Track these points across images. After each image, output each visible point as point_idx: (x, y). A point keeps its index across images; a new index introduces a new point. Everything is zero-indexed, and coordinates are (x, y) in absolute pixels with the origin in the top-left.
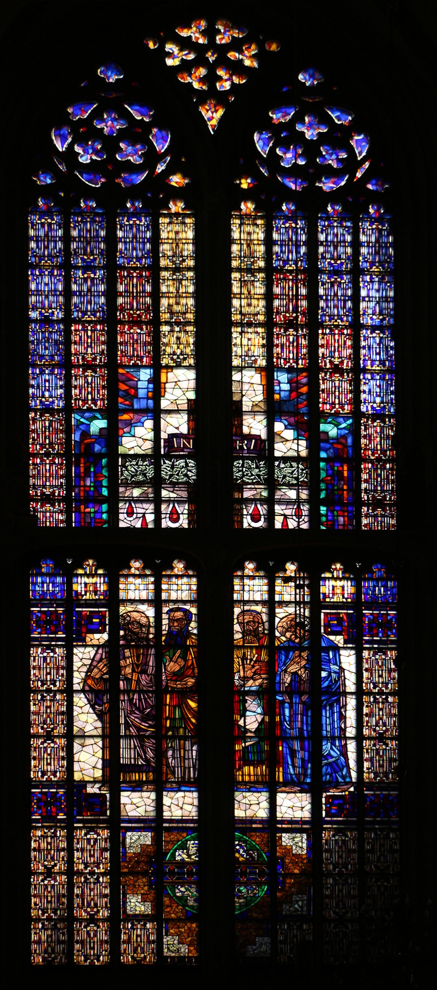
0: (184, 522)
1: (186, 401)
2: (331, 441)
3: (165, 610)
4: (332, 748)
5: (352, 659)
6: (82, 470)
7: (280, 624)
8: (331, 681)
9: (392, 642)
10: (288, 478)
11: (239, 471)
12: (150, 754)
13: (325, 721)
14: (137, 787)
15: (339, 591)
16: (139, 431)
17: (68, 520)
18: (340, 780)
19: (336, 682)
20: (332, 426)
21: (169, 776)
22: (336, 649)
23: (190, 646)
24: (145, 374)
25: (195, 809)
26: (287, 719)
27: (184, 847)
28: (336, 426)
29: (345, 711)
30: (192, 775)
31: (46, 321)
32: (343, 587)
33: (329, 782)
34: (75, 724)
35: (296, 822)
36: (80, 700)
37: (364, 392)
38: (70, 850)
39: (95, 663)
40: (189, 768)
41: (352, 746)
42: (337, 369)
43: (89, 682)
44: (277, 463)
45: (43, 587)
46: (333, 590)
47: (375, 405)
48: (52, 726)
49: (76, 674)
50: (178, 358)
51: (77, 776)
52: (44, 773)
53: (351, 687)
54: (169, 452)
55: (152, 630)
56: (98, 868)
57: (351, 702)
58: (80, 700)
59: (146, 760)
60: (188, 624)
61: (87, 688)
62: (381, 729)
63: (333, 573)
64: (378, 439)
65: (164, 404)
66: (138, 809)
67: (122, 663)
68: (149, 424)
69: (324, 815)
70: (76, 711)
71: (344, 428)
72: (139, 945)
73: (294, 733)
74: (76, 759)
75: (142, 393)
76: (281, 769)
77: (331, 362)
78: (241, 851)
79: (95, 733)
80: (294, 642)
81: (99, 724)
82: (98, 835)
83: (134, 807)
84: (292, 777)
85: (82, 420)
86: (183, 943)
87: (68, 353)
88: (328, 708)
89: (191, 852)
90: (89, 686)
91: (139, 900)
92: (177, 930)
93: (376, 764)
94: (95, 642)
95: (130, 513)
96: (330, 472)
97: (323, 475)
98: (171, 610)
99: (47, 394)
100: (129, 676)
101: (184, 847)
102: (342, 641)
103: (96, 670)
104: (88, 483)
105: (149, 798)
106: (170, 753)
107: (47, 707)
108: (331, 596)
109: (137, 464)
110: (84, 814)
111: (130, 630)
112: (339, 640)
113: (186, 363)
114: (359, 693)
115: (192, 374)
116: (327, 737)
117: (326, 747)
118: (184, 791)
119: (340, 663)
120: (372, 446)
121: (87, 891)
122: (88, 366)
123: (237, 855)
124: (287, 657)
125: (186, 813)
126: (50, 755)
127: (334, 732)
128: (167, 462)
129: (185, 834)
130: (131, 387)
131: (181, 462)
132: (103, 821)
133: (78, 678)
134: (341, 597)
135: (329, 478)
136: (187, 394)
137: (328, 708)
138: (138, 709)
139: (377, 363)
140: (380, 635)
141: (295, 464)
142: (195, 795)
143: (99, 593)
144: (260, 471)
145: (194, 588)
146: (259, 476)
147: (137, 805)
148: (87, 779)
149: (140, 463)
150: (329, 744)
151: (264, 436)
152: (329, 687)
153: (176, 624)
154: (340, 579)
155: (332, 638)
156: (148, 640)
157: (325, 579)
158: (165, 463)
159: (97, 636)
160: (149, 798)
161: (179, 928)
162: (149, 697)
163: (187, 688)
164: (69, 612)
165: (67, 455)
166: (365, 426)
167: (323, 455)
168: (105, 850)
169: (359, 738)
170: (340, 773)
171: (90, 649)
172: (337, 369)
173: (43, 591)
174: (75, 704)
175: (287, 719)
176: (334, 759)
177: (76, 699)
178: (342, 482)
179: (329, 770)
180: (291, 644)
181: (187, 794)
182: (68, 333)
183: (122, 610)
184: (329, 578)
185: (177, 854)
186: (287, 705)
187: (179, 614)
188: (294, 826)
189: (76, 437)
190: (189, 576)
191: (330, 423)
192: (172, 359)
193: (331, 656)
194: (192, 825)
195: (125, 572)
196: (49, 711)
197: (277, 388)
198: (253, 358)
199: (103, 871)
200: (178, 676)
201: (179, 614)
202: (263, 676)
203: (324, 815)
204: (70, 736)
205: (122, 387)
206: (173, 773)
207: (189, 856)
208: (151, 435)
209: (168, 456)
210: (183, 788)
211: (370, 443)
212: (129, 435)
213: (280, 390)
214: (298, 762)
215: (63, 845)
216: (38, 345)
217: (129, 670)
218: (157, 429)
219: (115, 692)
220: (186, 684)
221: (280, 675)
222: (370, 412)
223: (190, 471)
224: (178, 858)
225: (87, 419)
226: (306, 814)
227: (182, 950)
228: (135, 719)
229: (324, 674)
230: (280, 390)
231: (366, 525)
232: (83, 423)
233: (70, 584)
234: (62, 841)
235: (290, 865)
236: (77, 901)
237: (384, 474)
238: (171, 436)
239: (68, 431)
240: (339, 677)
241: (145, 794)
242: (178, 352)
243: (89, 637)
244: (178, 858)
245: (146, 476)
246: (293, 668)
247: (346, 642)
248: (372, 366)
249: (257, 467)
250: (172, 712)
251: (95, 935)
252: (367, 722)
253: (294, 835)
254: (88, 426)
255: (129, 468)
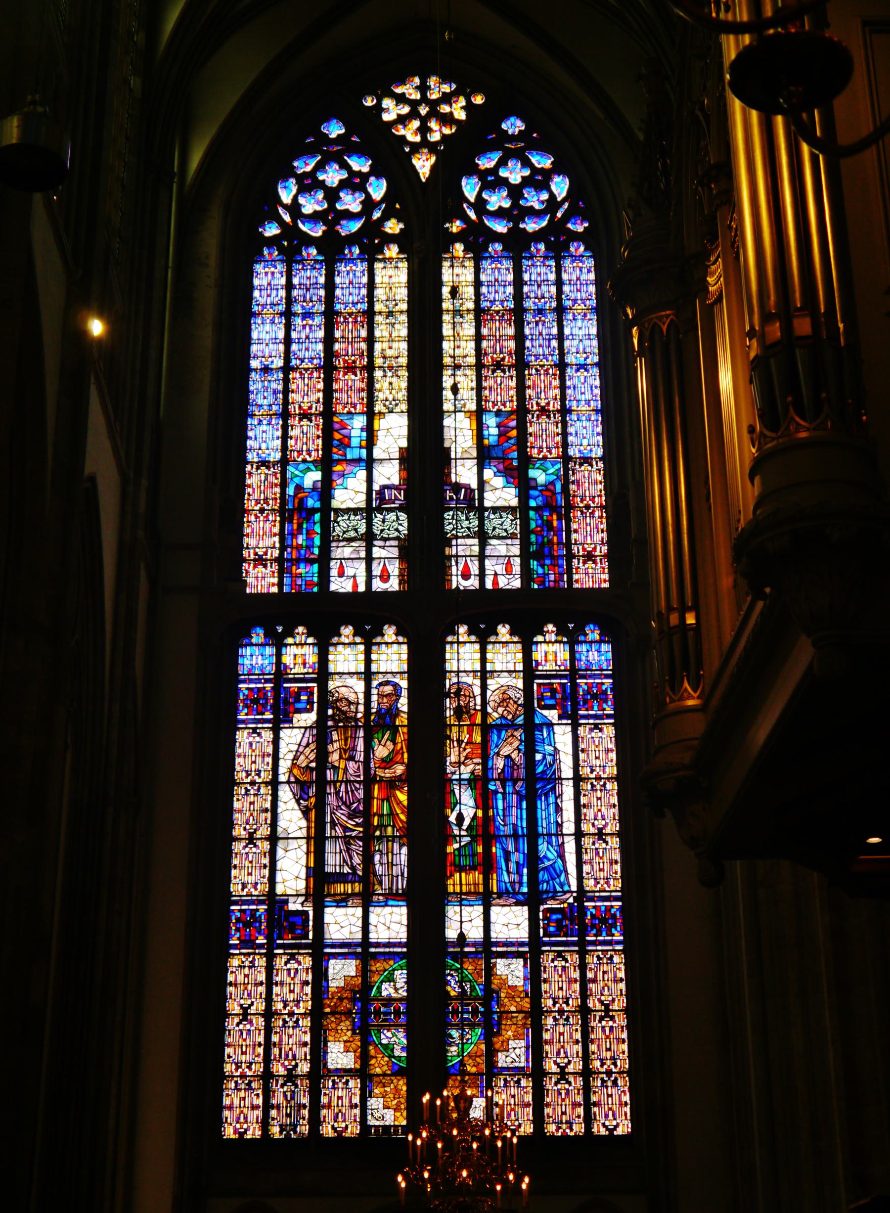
0: (393, 585)
1: (398, 449)
2: (540, 488)
3: (375, 683)
4: (548, 849)
5: (569, 737)
6: (295, 526)
7: (492, 698)
8: (546, 765)
9: (609, 716)
10: (497, 530)
11: (450, 524)
12: (357, 860)
13: (541, 814)
14: (342, 901)
15: (551, 657)
16: (351, 482)
17: (280, 585)
18: (558, 888)
19: (551, 766)
20: (541, 471)
21: (376, 887)
22: (550, 725)
23: (399, 726)
24: (359, 422)
25: (405, 929)
26: (501, 813)
27: (390, 979)
28: (545, 471)
29: (562, 801)
30: (400, 887)
31: (266, 370)
32: (556, 653)
33: (547, 892)
34: (279, 823)
35: (511, 944)
36: (285, 794)
37: (571, 434)
38: (270, 983)
39: (301, 749)
40: (397, 876)
41: (570, 846)
42: (544, 411)
43: (295, 771)
44: (486, 514)
45: (252, 660)
46: (546, 656)
47: (582, 448)
48: (255, 827)
49: (281, 762)
50: (391, 404)
51: (279, 890)
52: (244, 886)
53: (567, 771)
54: (380, 504)
55: (361, 708)
56: (298, 1007)
57: (568, 790)
58: (285, 794)
59: (353, 868)
60: (397, 700)
61: (292, 779)
62: (600, 824)
63: (544, 636)
64: (587, 484)
65: (377, 453)
66: (342, 930)
67: (330, 748)
68: (362, 474)
69: (541, 935)
70: (281, 807)
71: (552, 474)
72: (340, 1111)
73: (509, 830)
74: (278, 867)
75: (355, 442)
76: (495, 875)
77: (538, 404)
78: (453, 982)
79: (299, 834)
80: (506, 718)
81: (304, 823)
82: (299, 963)
83: (338, 927)
84: (506, 887)
85: (297, 472)
86: (389, 1108)
87: (286, 402)
88: (543, 798)
89: (398, 986)
90: (295, 777)
91: (342, 1050)
92: (382, 1090)
93: (596, 867)
94: (303, 724)
95: (341, 574)
96: (540, 522)
97: (533, 525)
98: (381, 684)
99: (264, 446)
100: (336, 764)
101: (390, 979)
102: (556, 717)
103: (302, 757)
104: (300, 542)
105: (353, 915)
106: (377, 858)
107: (251, 803)
108: (543, 663)
109: (349, 519)
110: (285, 937)
111: (339, 709)
112: (552, 715)
113: (397, 409)
114: (578, 779)
115: (404, 420)
116: (543, 835)
117: (543, 847)
118: (392, 906)
119: (555, 743)
120: (580, 493)
121: (285, 1038)
122: (305, 415)
123: (449, 988)
124: (499, 737)
125: (393, 935)
126: (251, 862)
127: (550, 829)
128: (378, 515)
129: (391, 962)
130: (345, 436)
131: (392, 516)
132: (306, 946)
133: (284, 765)
134: (554, 664)
135: (539, 529)
136: (398, 441)
137: (543, 798)
138: (344, 803)
139: (583, 403)
140: (596, 708)
141: (504, 515)
142: (404, 910)
143: (307, 665)
144: (470, 523)
145: (405, 657)
146: (468, 528)
147: (341, 925)
148: (289, 892)
149: (352, 517)
150: (546, 843)
151: (474, 485)
152: (544, 772)
153: (385, 700)
154: (553, 643)
155: (545, 712)
156: (356, 720)
157: (537, 643)
158: (376, 517)
159: (304, 716)
160: (353, 915)
161: (384, 1086)
162: (357, 789)
163: (395, 777)
164: (277, 690)
165: (282, 511)
166: (573, 470)
167: (533, 503)
168: (306, 983)
169: (579, 835)
170: (557, 880)
171: (296, 731)
172: (544, 411)
173: (251, 665)
174: (279, 799)
175: (501, 813)
176: (551, 862)
177: (280, 793)
178: (552, 533)
179: (546, 876)
180: (504, 722)
181: (395, 909)
182: (286, 381)
183: (332, 685)
184: (541, 642)
185: (383, 987)
186: (500, 796)
187: (388, 689)
188: (510, 949)
189: (290, 491)
190: (399, 643)
191: (538, 468)
192: (385, 405)
193: (545, 735)
194: (399, 950)
195: (335, 640)
196: (252, 808)
197: (486, 433)
198: (462, 402)
199: (303, 1011)
200: (387, 763)
201: (388, 689)
202: (475, 761)
203: (541, 935)
204: (273, 839)
205: (337, 436)
206: (380, 883)
207: (396, 990)
208: (363, 487)
209: (380, 510)
210: (391, 903)
211: (578, 489)
212: (341, 487)
213: (489, 435)
214: (513, 867)
215: (262, 977)
216: (257, 394)
217: (335, 757)
218: (370, 480)
219: (322, 783)
220: (395, 772)
221: (493, 758)
222: (578, 455)
223: (401, 525)
224: (384, 993)
225: (301, 472)
226: (522, 933)
227: (387, 1117)
228: (341, 815)
229: (538, 757)
230: (489, 435)
231: (577, 581)
232: (297, 476)
233: (279, 655)
234: (260, 972)
235: (506, 1000)
236: (276, 1051)
237: (593, 522)
238: (384, 487)
239: (284, 485)
240: (554, 760)
241: (350, 911)
242: (390, 398)
243: (297, 717)
244: (384, 993)
245: (357, 532)
246: (505, 751)
247: (560, 717)
248: (578, 407)
249: (467, 519)
250: (380, 807)
251: (292, 1098)
252: (585, 815)
253: (509, 961)
254: (302, 478)
255: (341, 523)
